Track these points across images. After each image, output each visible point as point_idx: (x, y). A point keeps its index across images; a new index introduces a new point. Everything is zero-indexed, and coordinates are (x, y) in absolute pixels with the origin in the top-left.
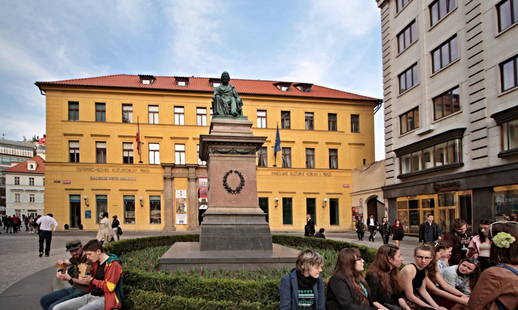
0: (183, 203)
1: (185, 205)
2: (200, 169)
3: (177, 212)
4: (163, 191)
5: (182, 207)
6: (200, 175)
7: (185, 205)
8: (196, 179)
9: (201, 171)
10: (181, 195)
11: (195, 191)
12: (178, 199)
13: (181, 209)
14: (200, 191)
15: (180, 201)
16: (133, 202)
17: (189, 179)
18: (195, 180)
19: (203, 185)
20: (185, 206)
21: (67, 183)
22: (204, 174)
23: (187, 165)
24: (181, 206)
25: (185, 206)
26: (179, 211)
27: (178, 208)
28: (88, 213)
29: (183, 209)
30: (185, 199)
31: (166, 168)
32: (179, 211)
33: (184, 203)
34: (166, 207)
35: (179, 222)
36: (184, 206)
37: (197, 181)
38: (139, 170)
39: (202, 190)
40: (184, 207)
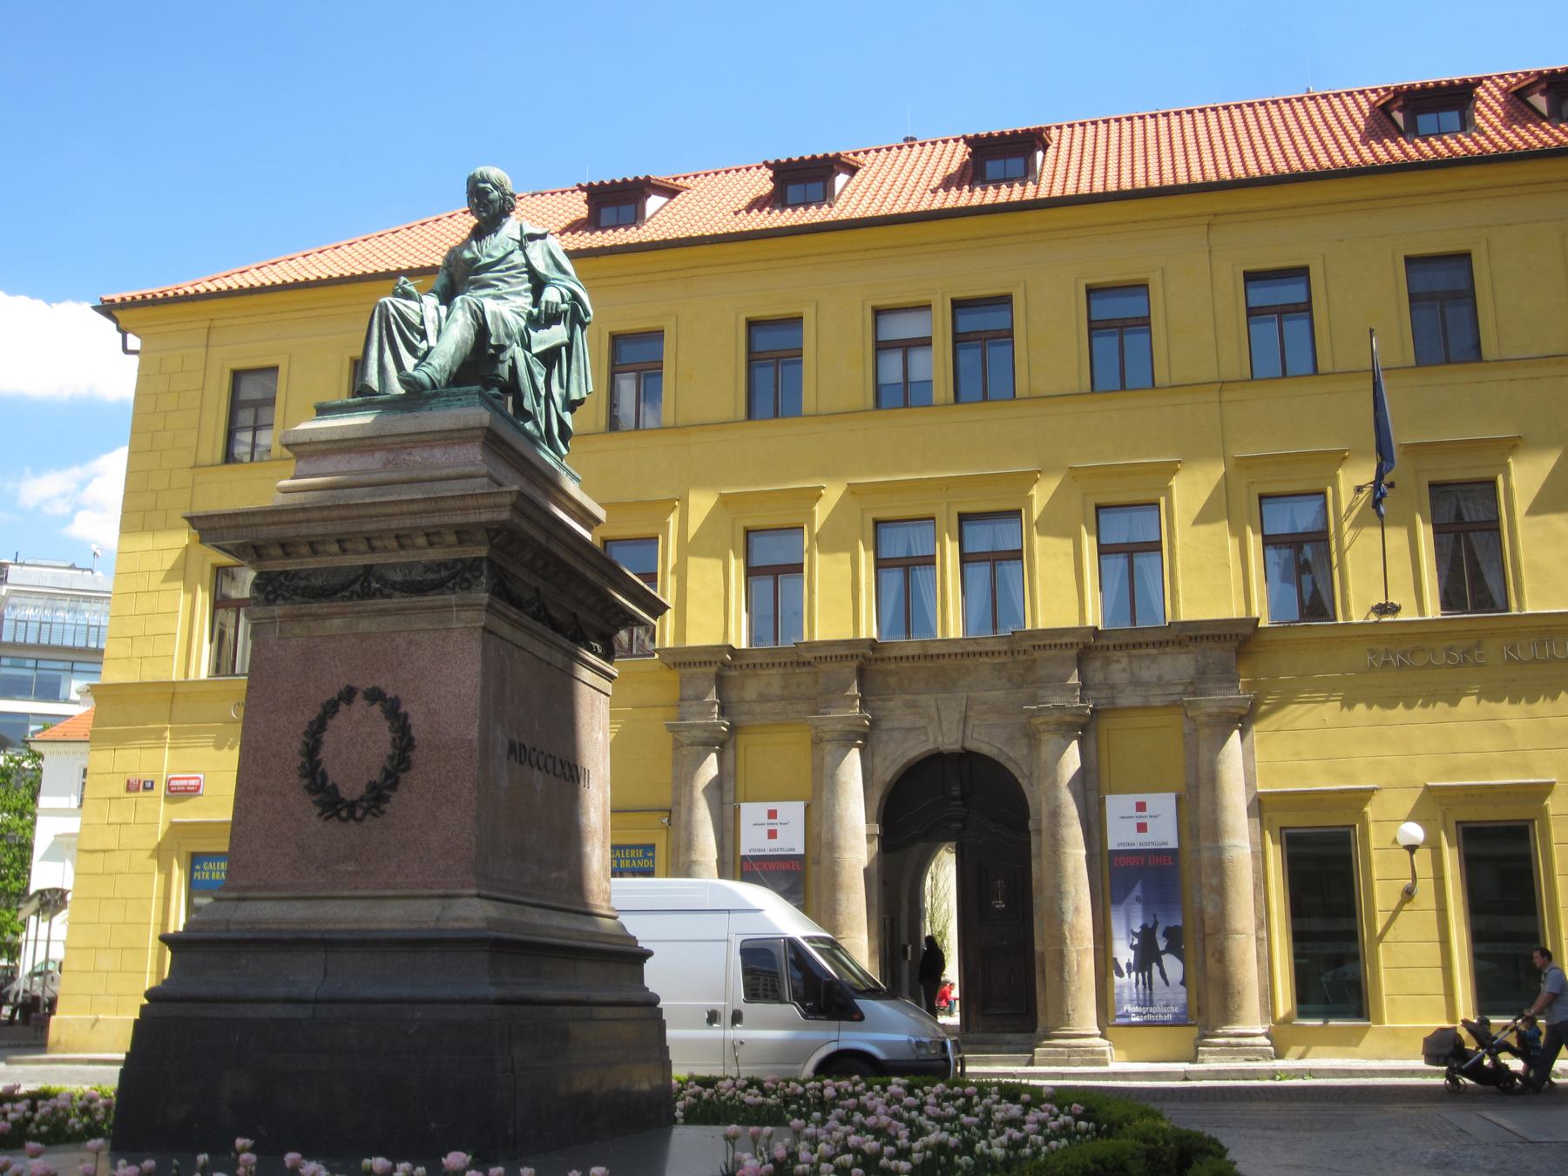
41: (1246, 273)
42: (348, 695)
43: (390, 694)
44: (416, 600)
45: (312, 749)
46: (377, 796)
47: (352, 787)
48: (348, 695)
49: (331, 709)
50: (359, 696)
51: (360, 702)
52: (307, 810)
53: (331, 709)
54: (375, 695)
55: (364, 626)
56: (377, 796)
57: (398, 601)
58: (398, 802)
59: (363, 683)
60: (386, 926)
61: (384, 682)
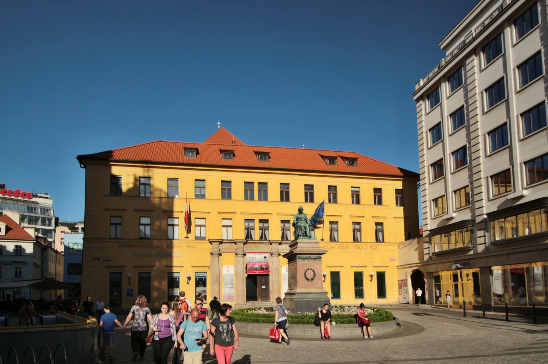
4: (210, 267)
6: (248, 250)
14: (248, 266)
16: (178, 279)
17: (236, 254)
18: (243, 256)
19: (251, 261)
21: (108, 261)
23: (235, 241)
31: (213, 243)
34: (213, 284)
38: (184, 245)
39: (250, 266)
42: (308, 269)
43: (313, 269)
44: (314, 260)
45: (305, 274)
46: (312, 279)
47: (310, 278)
48: (308, 269)
49: (307, 270)
50: (309, 269)
51: (310, 270)
52: (305, 280)
53: (307, 270)
54: (311, 269)
55: (309, 262)
56: (312, 279)
57: (313, 260)
58: (314, 280)
59: (310, 268)
61: (312, 268)
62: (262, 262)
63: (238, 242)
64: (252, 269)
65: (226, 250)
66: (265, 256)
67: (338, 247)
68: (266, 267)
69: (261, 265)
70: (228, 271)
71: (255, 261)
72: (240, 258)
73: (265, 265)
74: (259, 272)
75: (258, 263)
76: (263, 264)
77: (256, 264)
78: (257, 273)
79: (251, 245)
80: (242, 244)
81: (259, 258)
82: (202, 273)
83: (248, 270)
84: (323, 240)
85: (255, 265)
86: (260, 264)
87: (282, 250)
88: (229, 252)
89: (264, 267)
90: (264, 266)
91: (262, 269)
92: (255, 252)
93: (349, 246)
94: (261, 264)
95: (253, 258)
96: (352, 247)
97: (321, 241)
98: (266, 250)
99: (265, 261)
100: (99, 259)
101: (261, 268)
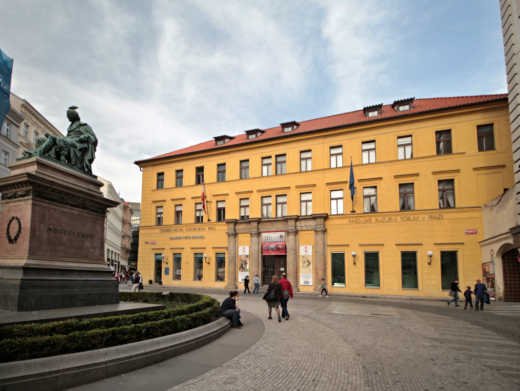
0: (245, 260)
1: (248, 262)
2: (264, 223)
3: (240, 269)
5: (244, 264)
6: (263, 229)
7: (247, 262)
8: (259, 234)
9: (264, 225)
10: (244, 252)
11: (256, 247)
12: (241, 256)
13: (244, 266)
14: (263, 246)
15: (243, 258)
17: (251, 234)
19: (267, 240)
20: (247, 263)
22: (267, 228)
24: (244, 263)
25: (247, 263)
26: (241, 269)
27: (240, 265)
28: (167, 270)
29: (246, 266)
30: (247, 256)
32: (241, 269)
33: (247, 259)
35: (241, 280)
36: (246, 263)
37: (260, 236)
40: (246, 264)
41: (330, 147)
60: (12, 264)
62: (277, 242)
63: (253, 221)
64: (268, 250)
65: (242, 230)
66: (281, 235)
67: (376, 220)
68: (282, 248)
69: (277, 245)
70: (244, 252)
71: (271, 240)
72: (255, 239)
73: (281, 245)
74: (275, 253)
75: (274, 242)
76: (280, 244)
77: (272, 244)
78: (273, 254)
79: (266, 224)
80: (255, 224)
81: (275, 236)
82: (200, 255)
83: (264, 250)
84: (353, 212)
85: (271, 245)
86: (276, 244)
87: (300, 227)
88: (245, 232)
89: (280, 248)
90: (281, 246)
91: (278, 249)
92: (270, 231)
93: (393, 217)
94: (277, 244)
95: (269, 237)
96: (399, 219)
97: (351, 213)
98: (282, 228)
99: (281, 240)
100: (148, 243)
101: (277, 248)
